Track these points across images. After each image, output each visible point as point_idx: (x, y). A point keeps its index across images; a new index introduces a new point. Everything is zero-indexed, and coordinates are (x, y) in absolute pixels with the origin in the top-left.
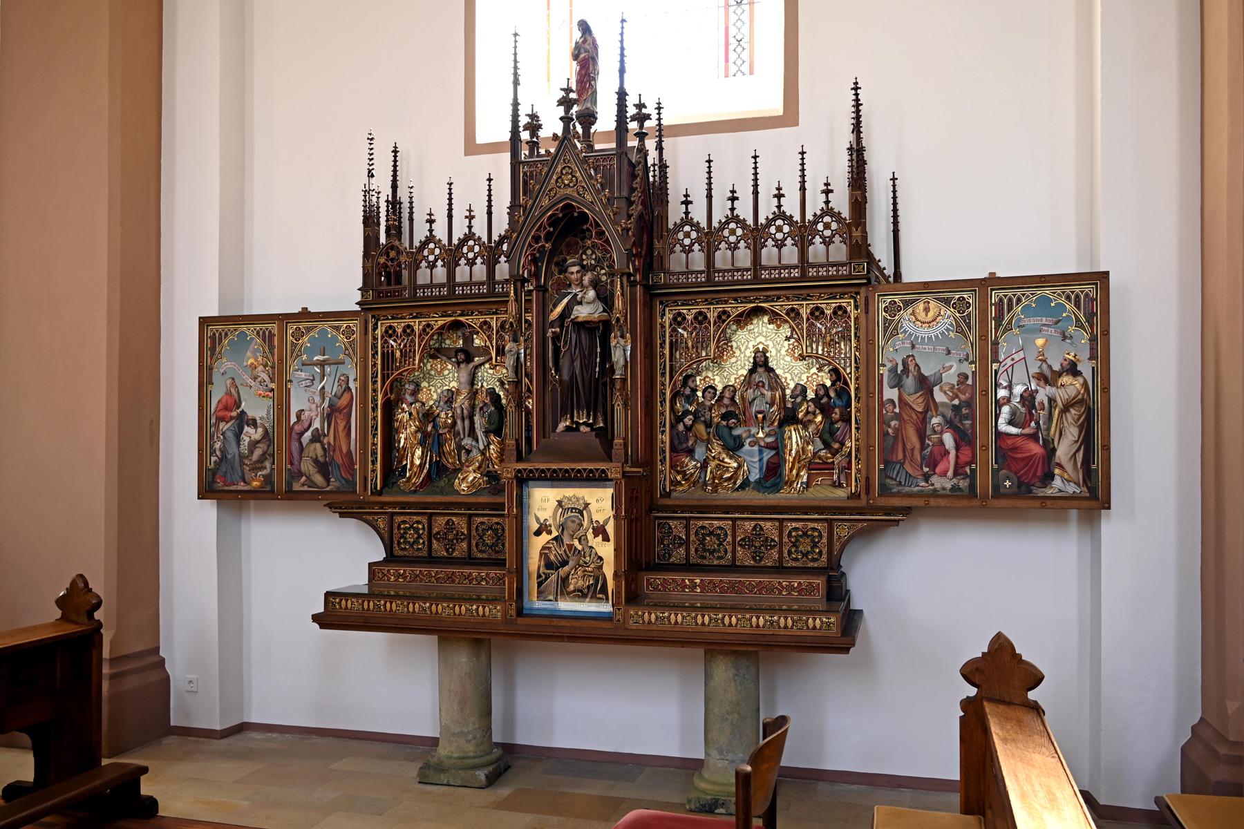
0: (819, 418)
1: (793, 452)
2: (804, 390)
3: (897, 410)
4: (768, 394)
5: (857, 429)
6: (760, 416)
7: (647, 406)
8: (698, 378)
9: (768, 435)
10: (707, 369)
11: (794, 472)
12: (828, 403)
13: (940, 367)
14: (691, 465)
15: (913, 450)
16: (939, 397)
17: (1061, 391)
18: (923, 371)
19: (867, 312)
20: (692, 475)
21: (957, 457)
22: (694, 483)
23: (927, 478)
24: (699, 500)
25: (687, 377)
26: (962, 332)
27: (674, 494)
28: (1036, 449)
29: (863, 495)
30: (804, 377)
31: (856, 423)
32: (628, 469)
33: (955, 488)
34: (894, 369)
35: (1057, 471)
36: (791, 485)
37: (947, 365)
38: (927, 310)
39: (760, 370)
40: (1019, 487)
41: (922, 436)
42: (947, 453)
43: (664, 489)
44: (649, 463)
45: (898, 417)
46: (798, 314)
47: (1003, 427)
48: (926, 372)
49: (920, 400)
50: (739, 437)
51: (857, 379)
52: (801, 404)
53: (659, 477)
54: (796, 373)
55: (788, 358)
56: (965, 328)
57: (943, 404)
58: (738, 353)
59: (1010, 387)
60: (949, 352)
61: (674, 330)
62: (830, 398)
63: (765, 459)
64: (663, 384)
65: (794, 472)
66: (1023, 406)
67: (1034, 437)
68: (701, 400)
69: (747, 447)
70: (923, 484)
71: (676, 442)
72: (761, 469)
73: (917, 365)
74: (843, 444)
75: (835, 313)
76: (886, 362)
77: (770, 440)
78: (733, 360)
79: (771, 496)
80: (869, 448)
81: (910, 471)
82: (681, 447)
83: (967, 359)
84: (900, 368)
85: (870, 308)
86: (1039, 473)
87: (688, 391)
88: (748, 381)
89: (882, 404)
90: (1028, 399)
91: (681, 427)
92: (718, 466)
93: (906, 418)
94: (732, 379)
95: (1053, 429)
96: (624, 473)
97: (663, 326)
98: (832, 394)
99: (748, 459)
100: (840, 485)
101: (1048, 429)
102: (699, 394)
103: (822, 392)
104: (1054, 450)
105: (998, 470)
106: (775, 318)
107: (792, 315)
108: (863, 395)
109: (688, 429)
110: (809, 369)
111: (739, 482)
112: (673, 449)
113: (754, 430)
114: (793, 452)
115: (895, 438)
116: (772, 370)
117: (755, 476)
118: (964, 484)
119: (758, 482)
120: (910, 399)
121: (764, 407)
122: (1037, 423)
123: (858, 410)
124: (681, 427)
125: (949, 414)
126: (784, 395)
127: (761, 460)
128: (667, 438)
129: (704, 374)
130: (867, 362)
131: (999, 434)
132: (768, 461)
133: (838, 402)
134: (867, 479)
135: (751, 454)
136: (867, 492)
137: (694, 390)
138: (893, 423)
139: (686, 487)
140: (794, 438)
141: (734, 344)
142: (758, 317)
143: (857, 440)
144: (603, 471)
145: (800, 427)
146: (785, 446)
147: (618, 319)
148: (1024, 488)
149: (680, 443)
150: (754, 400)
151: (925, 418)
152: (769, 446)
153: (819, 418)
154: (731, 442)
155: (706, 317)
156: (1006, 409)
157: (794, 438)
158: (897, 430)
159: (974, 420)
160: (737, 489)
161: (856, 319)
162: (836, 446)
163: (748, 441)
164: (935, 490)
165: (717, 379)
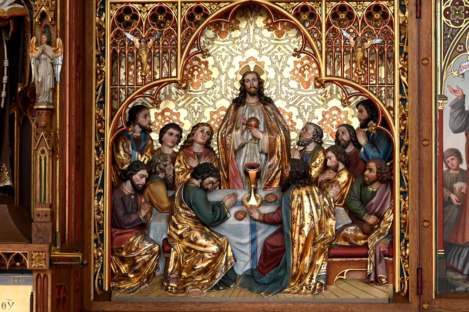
0: (344, 177)
1: (306, 229)
2: (319, 133)
3: (464, 166)
4: (265, 138)
5: (404, 194)
6: (252, 172)
7: (77, 154)
8: (153, 112)
9: (264, 202)
10: (168, 98)
11: (307, 260)
12: (356, 153)
14: (143, 248)
19: (419, 17)
20: (145, 264)
22: (149, 277)
24: (157, 304)
25: (136, 110)
27: (116, 295)
29: (412, 295)
30: (318, 113)
31: (402, 184)
32: (57, 254)
36: (301, 280)
39: (252, 100)
43: (101, 286)
44: (79, 242)
46: (313, 15)
50: (220, 204)
51: (403, 117)
52: (314, 155)
53: (94, 267)
54: (311, 106)
55: (293, 84)
58: (215, 74)
61: (118, 35)
62: (358, 146)
63: (260, 240)
64: (101, 120)
65: (307, 260)
68: (157, 145)
69: (231, 221)
71: (121, 213)
72: (253, 255)
74: (381, 217)
75: (369, 15)
76: (447, 92)
77: (267, 210)
78: (209, 84)
79: (270, 297)
80: (422, 224)
82: (127, 220)
87: (137, 132)
88: (232, 118)
89: (441, 157)
91: (127, 188)
92: (187, 250)
94: (207, 113)
96: (51, 260)
97: (101, 29)
98: (362, 140)
99: (233, 239)
100: (377, 281)
102: (155, 136)
103: (346, 137)
106: (275, 19)
107: (305, 17)
108: (412, 142)
109: (139, 191)
110: (326, 101)
111: (219, 276)
112: (115, 223)
113: (242, 194)
114: (306, 229)
116: (267, 101)
117: (243, 266)
119: (250, 276)
121: (258, 159)
123: (404, 165)
124: (127, 188)
126: (288, 140)
127: (253, 241)
128: (105, 204)
129: (162, 106)
130: (421, 91)
132: (266, 243)
133: (372, 153)
134: (419, 271)
135: (238, 232)
136: (420, 291)
137: (146, 131)
138: (458, 186)
139: (134, 283)
140: (307, 208)
141: (210, 60)
142: (247, 18)
143: (404, 211)
144: (18, 257)
145: (315, 190)
146: (294, 220)
147: (44, 15)
149: (127, 213)
150: (242, 146)
152: (267, 220)
153: (344, 177)
154: (208, 212)
155: (169, 16)
157: (307, 208)
160: (217, 287)
161: (403, 26)
162: (371, 220)
163: (233, 211)
165: (183, 113)
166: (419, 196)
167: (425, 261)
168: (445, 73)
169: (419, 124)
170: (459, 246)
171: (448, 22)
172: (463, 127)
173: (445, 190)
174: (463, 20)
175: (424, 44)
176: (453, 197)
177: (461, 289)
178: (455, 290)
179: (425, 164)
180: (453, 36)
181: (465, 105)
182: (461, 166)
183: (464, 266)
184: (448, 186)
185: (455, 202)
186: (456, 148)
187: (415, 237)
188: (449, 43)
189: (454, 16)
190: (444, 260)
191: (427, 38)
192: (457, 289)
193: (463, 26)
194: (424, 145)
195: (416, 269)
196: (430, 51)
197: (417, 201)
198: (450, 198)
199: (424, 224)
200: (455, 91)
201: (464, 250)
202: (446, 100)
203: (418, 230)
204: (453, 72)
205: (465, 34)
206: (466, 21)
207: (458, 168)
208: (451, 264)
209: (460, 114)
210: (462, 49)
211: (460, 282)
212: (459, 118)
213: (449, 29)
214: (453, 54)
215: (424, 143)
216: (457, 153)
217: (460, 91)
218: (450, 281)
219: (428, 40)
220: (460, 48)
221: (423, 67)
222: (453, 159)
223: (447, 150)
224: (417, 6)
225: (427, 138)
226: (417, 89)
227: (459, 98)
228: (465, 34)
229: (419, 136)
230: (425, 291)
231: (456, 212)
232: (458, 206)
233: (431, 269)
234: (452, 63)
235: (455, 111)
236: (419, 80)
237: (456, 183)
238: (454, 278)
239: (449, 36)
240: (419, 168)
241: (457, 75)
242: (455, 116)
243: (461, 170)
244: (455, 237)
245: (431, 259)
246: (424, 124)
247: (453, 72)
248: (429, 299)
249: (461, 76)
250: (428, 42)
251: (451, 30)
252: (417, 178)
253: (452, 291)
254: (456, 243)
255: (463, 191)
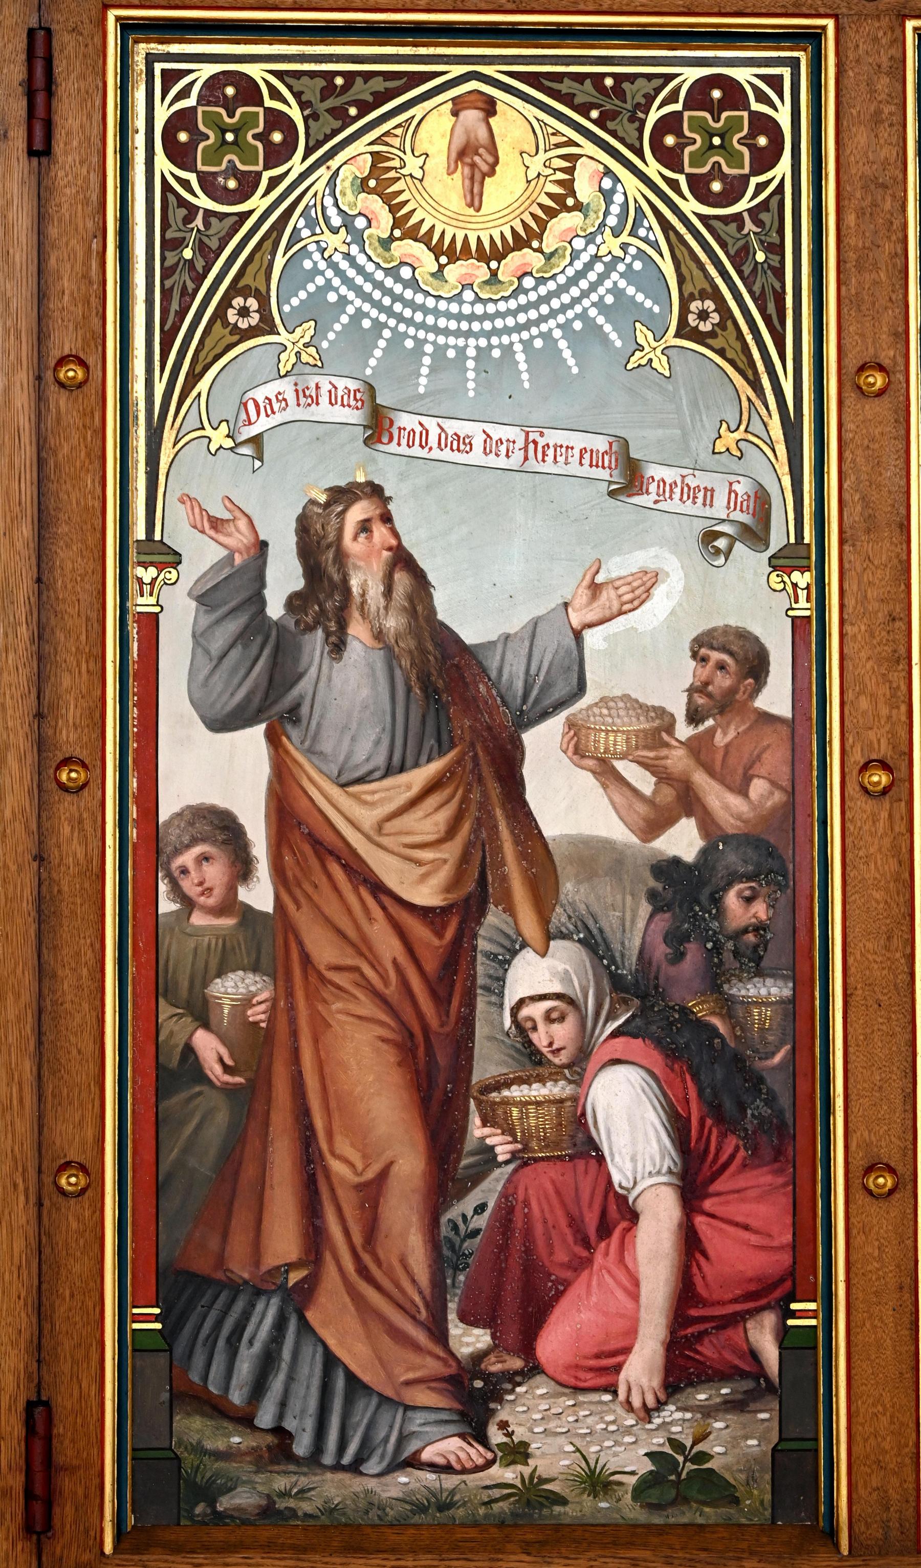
3: (260, 895)
13: (568, 584)
15: (373, 1191)
16: (565, 800)
18: (447, 606)
21: (690, 1244)
23: (474, 1400)
26: (721, 337)
33: (675, 1478)
34: (236, 589)
37: (616, 568)
38: (475, 161)
41: (440, 1090)
42: (619, 1213)
45: (267, 943)
48: (471, 612)
49: (429, 821)
56: (743, 306)
57: (594, 855)
60: (631, 478)
70: (450, 1447)
73: (402, 559)
76: (178, 530)
81: (355, 1353)
83: (755, 534)
84: (284, 578)
85: (69, 118)
89: (149, 848)
93: (325, 950)
115: (249, 1099)
118: (736, 1443)
120: (353, 814)
125: (635, 926)
151: (458, 956)
158: (257, 1048)
159: (808, 974)
164: (535, 1495)
166: (40, 1043)
167: (66, 1368)
168: (168, 436)
169: (41, 680)
170: (235, 1288)
171: (185, 184)
172: (259, 696)
173: (165, 1010)
174: (259, 175)
175: (67, 283)
176: (207, 1046)
177: (242, 1499)
178: (212, 1503)
179: (67, 882)
180: (208, 254)
181: (267, 593)
182: (244, 895)
183: (258, 1389)
184: (184, 992)
185: (215, 1071)
186: (221, 802)
187: (19, 1245)
188: (190, 286)
189: (214, 155)
190: (162, 1360)
191: (80, 254)
192: (224, 1504)
193: (257, 203)
194: (62, 787)
195: (21, 1405)
196: (96, 321)
197: (28, 1067)
198: (189, 1050)
199: (63, 1182)
200: (216, 524)
201: (260, 1307)
202: (176, 564)
203: (33, 1211)
204: (208, 431)
205: (268, 244)
206: (274, 182)
207: (229, 905)
208: (195, 1377)
209: (242, 637)
210: (254, 319)
211: (241, 1469)
212: (235, 654)
213: (188, 219)
214: (209, 343)
215: (64, 777)
216: (225, 828)
217: (242, 524)
218: (189, 1460)
219: (86, 264)
220: (244, 312)
221: (60, 401)
222: (205, 858)
223: (179, 815)
224: (31, 95)
225: (78, 752)
226: (30, 510)
227: (238, 560)
228: (268, 244)
229: (41, 744)
230: (64, 1514)
231: (222, 1118)
232: (229, 1091)
233: (94, 1404)
234: (203, 385)
235: (218, 622)
236: (41, 463)
237: (219, 974)
238: (209, 1445)
239: (188, 254)
240: (40, 900)
241: (229, 443)
242: (218, 643)
243: (248, 914)
244: (214, 1244)
245: (95, 1357)
246: (66, 681)
247: (208, 431)
248: (86, 1557)
249: (246, 450)
250: (86, 276)
251: (199, 222)
252: (29, 952)
253: (199, 1510)
254: (219, 1275)
255: (258, 1014)
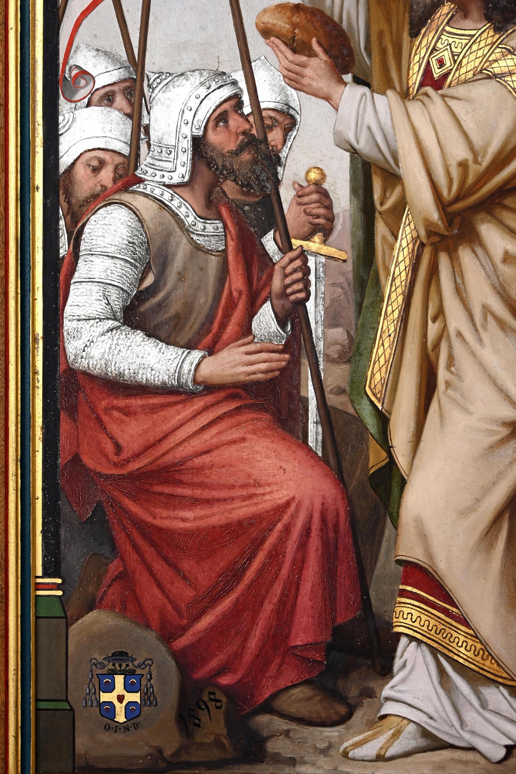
17: (429, 117)
28: (283, 476)
35: (409, 615)
40: (187, 716)
47: (100, 344)
59: (132, 94)
66: (211, 206)
67: (271, 399)
86: (304, 632)
90: (239, 166)
95: (382, 351)
101: (355, 353)
104: (389, 483)
105: (66, 613)
122: (293, 316)
131: (69, 388)
148: (213, 725)
156: (109, 230)
